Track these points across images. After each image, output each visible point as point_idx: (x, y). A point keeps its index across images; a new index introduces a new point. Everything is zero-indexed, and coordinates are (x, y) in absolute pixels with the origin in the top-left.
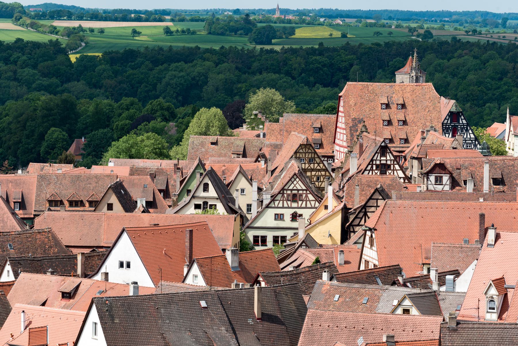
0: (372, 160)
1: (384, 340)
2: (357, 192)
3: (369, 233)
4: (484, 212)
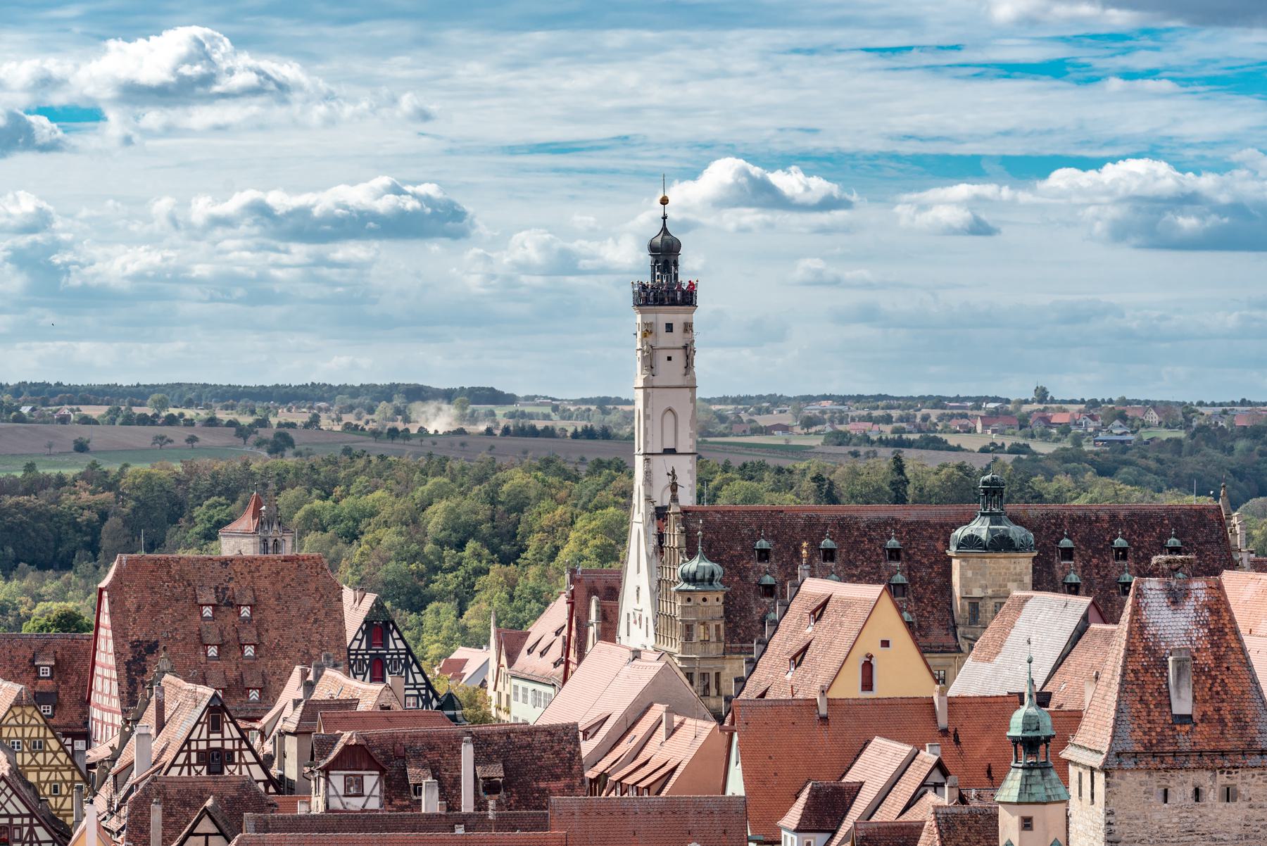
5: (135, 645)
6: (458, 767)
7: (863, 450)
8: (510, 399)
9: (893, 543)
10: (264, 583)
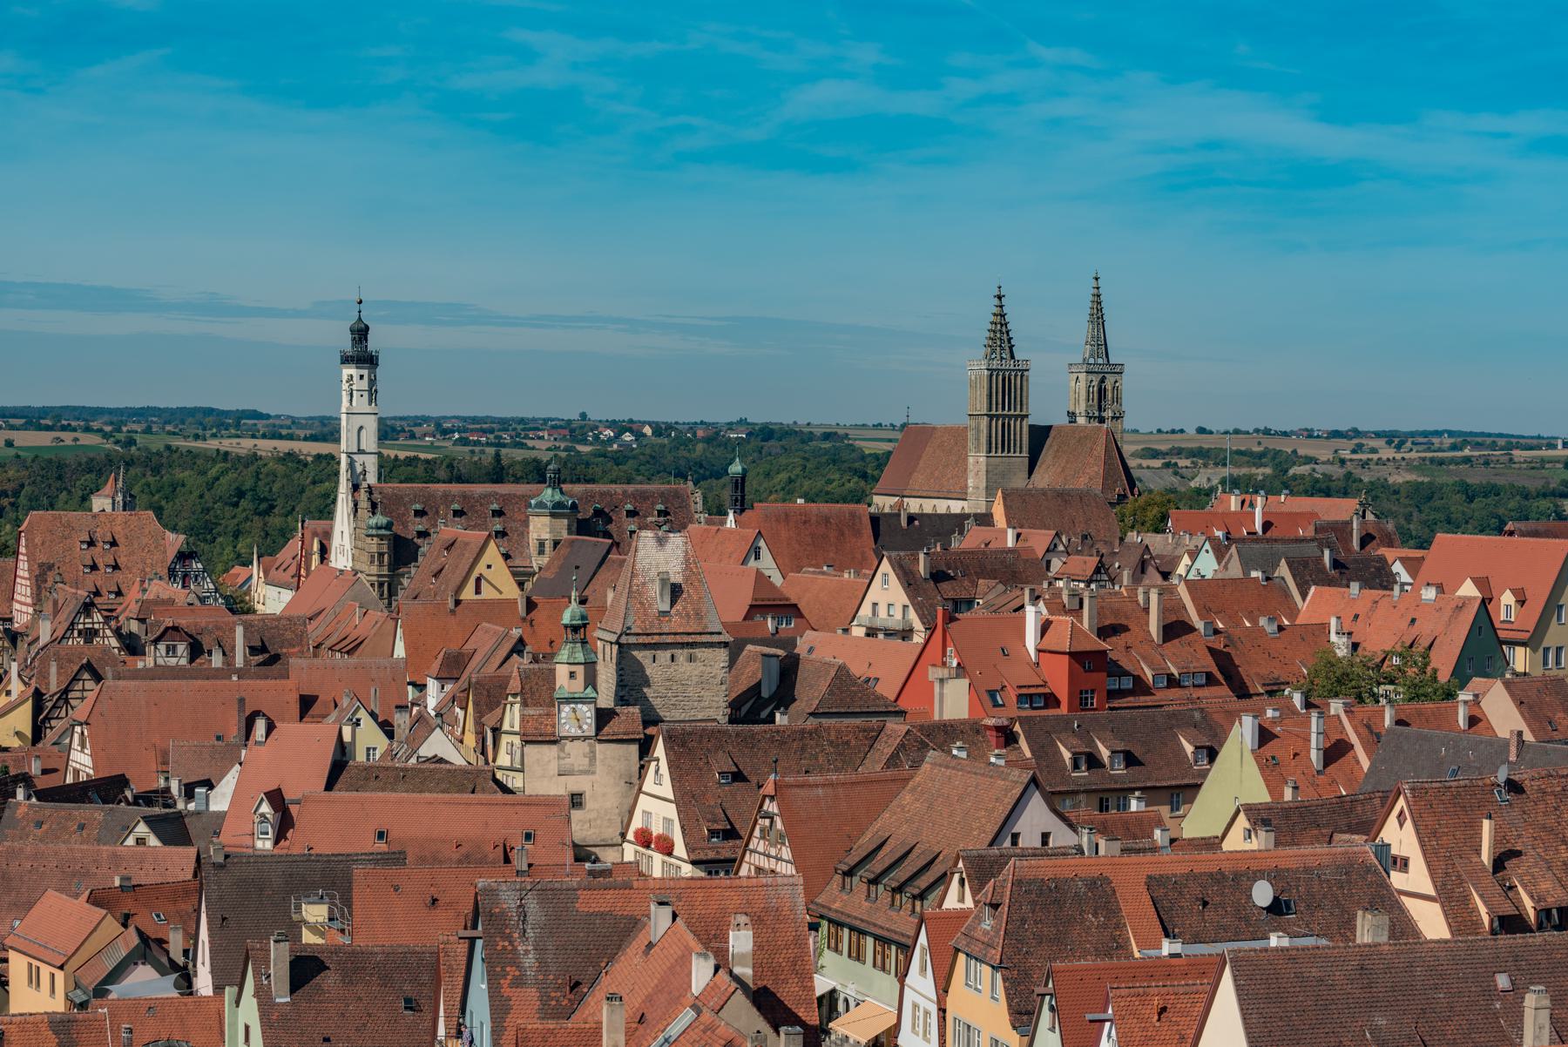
0: (72, 624)
1: (117, 883)
2: (53, 669)
3: (78, 729)
4: (243, 694)
5: (41, 565)
6: (234, 639)
7: (477, 449)
8: (268, 417)
9: (495, 506)
10: (119, 528)
